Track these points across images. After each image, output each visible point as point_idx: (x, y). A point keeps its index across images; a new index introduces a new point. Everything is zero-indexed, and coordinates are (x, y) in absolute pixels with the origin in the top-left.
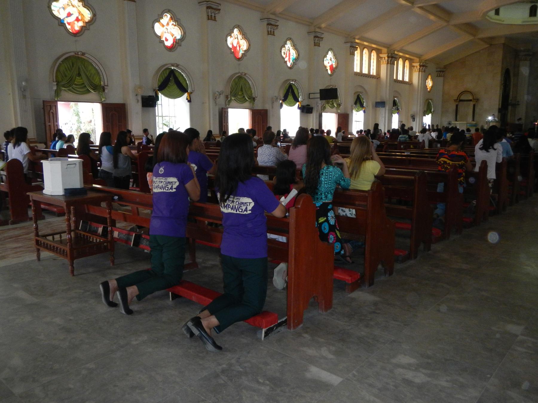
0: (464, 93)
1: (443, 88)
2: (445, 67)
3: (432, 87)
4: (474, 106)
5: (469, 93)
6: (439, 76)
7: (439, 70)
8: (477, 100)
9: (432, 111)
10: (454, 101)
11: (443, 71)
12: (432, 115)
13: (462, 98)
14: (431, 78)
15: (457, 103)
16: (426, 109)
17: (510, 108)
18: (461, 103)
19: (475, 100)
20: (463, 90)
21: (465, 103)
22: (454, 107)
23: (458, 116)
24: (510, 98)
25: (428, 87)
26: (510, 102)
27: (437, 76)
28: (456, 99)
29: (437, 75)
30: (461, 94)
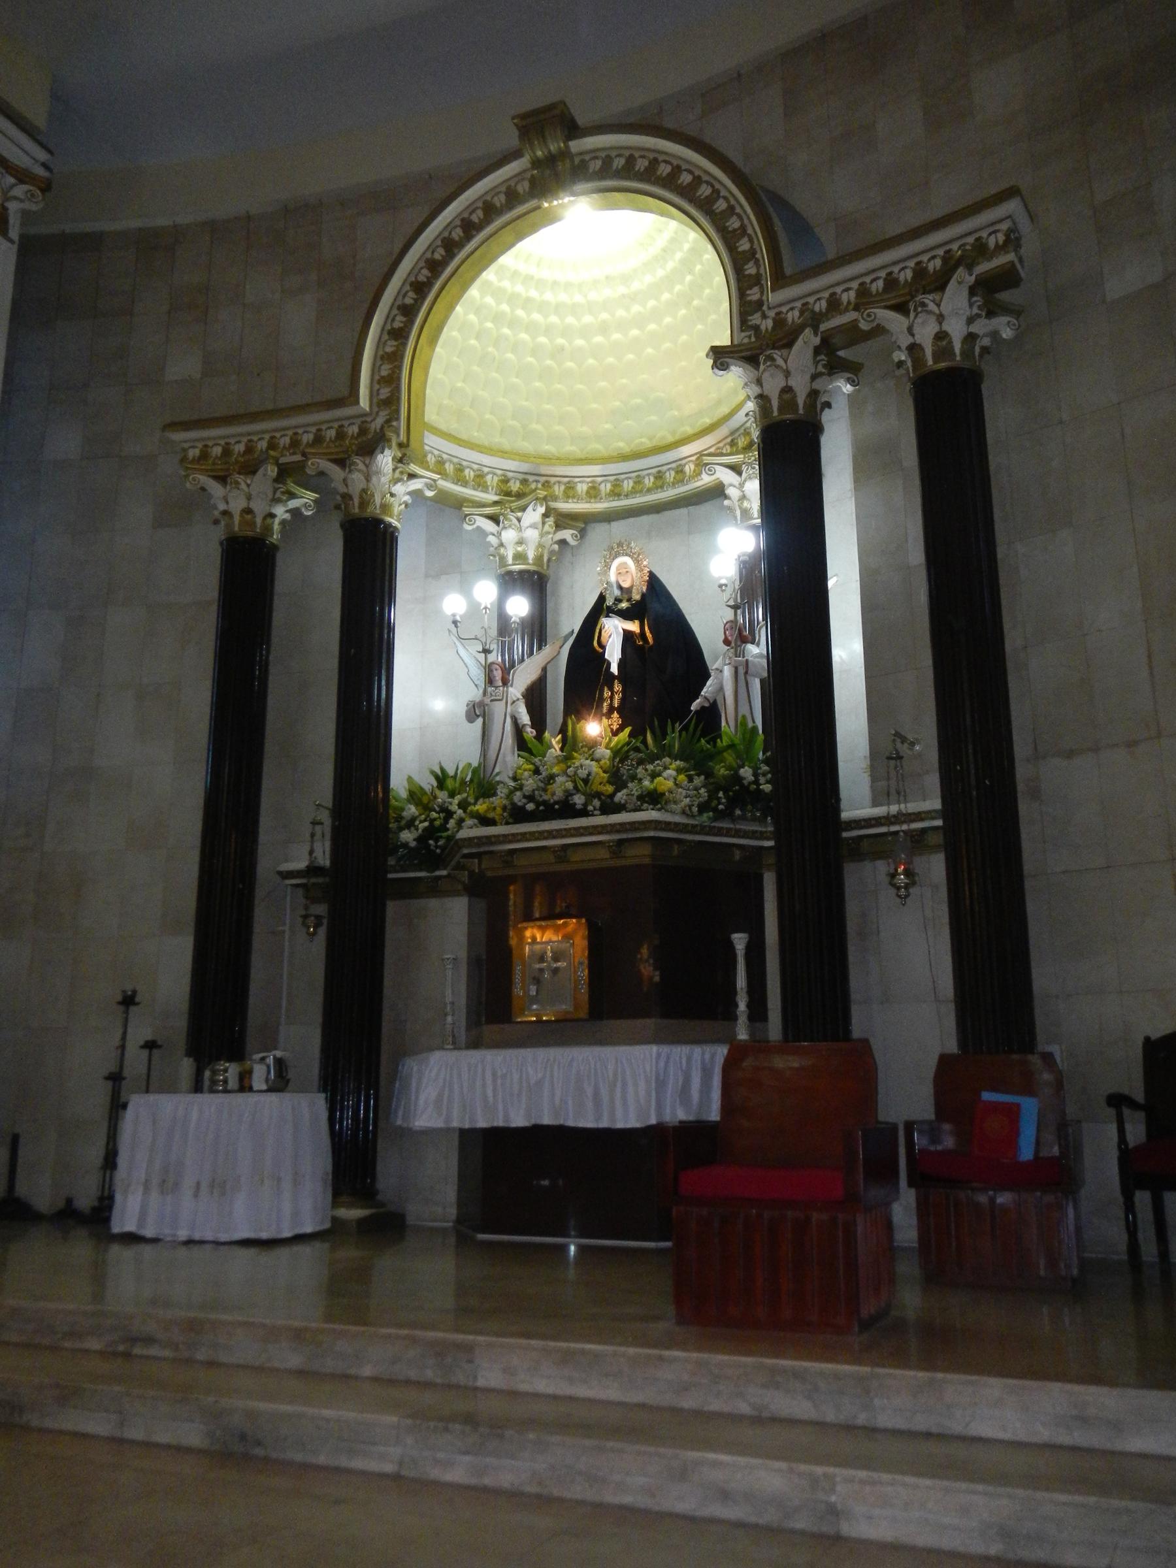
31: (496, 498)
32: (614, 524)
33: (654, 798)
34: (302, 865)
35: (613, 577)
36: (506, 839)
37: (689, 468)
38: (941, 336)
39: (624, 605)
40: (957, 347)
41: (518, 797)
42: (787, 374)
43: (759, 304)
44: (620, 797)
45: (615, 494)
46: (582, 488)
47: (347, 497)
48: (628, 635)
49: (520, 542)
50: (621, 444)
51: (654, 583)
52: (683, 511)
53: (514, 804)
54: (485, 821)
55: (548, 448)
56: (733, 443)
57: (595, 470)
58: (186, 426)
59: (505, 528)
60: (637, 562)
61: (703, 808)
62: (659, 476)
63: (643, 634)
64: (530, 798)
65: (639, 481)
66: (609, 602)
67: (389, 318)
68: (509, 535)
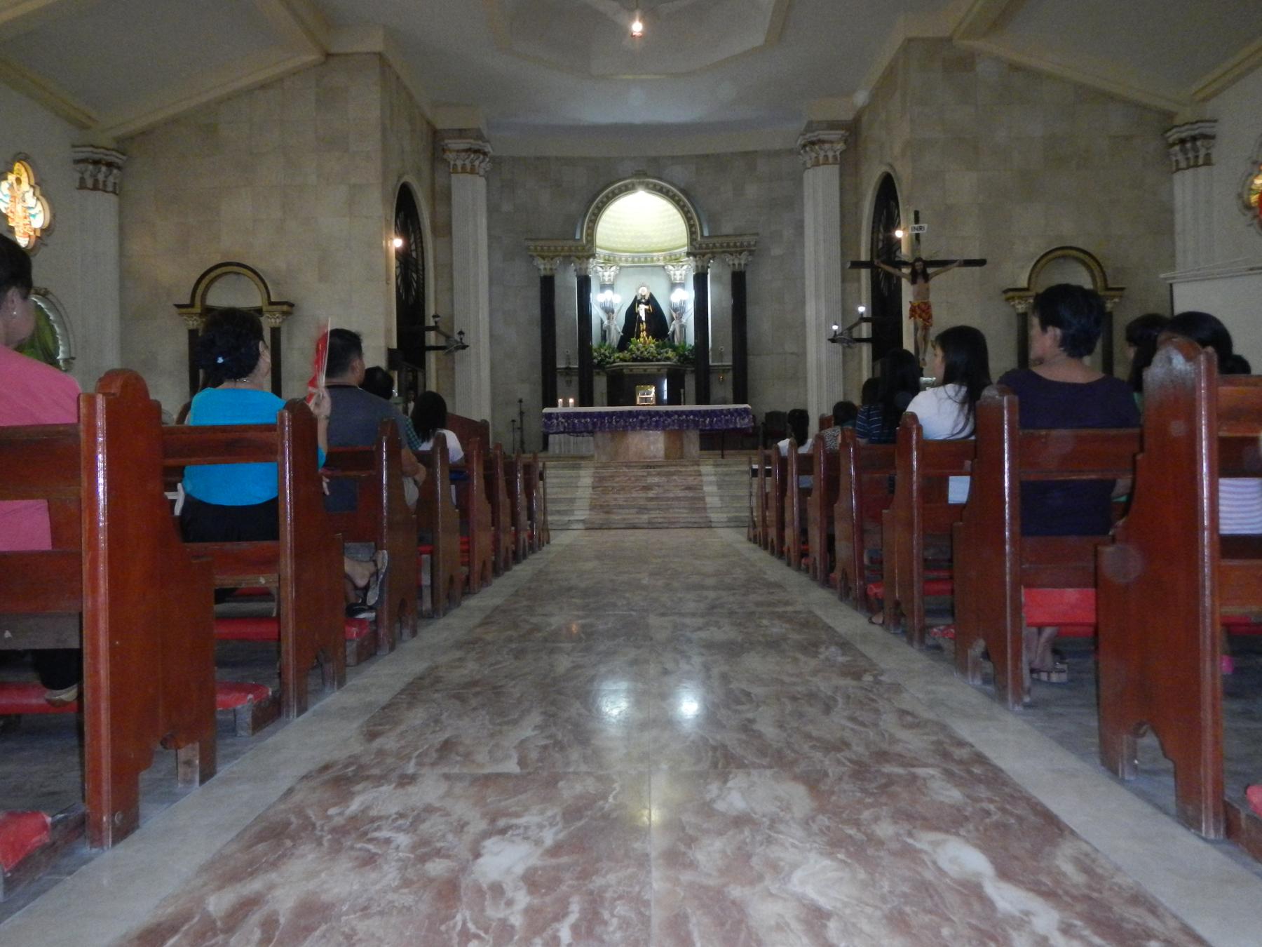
0: (226, 273)
1: (122, 253)
2: (124, 144)
3: (46, 231)
6: (90, 183)
7: (86, 153)
8: (285, 308)
9: (61, 356)
10: (175, 308)
11: (110, 165)
17: (431, 359)
20: (218, 260)
24: (431, 309)
26: (431, 322)
27: (82, 186)
28: (187, 302)
29: (82, 180)
33: (668, 359)
34: (563, 366)
35: (640, 292)
36: (631, 366)
37: (655, 258)
38: (740, 264)
39: (643, 301)
42: (703, 261)
43: (696, 240)
44: (659, 357)
46: (623, 259)
47: (580, 269)
48: (646, 310)
49: (610, 276)
50: (633, 246)
51: (651, 296)
53: (633, 358)
56: (670, 256)
57: (628, 254)
61: (679, 360)
62: (646, 259)
64: (638, 356)
65: (639, 258)
66: (639, 298)
68: (605, 273)
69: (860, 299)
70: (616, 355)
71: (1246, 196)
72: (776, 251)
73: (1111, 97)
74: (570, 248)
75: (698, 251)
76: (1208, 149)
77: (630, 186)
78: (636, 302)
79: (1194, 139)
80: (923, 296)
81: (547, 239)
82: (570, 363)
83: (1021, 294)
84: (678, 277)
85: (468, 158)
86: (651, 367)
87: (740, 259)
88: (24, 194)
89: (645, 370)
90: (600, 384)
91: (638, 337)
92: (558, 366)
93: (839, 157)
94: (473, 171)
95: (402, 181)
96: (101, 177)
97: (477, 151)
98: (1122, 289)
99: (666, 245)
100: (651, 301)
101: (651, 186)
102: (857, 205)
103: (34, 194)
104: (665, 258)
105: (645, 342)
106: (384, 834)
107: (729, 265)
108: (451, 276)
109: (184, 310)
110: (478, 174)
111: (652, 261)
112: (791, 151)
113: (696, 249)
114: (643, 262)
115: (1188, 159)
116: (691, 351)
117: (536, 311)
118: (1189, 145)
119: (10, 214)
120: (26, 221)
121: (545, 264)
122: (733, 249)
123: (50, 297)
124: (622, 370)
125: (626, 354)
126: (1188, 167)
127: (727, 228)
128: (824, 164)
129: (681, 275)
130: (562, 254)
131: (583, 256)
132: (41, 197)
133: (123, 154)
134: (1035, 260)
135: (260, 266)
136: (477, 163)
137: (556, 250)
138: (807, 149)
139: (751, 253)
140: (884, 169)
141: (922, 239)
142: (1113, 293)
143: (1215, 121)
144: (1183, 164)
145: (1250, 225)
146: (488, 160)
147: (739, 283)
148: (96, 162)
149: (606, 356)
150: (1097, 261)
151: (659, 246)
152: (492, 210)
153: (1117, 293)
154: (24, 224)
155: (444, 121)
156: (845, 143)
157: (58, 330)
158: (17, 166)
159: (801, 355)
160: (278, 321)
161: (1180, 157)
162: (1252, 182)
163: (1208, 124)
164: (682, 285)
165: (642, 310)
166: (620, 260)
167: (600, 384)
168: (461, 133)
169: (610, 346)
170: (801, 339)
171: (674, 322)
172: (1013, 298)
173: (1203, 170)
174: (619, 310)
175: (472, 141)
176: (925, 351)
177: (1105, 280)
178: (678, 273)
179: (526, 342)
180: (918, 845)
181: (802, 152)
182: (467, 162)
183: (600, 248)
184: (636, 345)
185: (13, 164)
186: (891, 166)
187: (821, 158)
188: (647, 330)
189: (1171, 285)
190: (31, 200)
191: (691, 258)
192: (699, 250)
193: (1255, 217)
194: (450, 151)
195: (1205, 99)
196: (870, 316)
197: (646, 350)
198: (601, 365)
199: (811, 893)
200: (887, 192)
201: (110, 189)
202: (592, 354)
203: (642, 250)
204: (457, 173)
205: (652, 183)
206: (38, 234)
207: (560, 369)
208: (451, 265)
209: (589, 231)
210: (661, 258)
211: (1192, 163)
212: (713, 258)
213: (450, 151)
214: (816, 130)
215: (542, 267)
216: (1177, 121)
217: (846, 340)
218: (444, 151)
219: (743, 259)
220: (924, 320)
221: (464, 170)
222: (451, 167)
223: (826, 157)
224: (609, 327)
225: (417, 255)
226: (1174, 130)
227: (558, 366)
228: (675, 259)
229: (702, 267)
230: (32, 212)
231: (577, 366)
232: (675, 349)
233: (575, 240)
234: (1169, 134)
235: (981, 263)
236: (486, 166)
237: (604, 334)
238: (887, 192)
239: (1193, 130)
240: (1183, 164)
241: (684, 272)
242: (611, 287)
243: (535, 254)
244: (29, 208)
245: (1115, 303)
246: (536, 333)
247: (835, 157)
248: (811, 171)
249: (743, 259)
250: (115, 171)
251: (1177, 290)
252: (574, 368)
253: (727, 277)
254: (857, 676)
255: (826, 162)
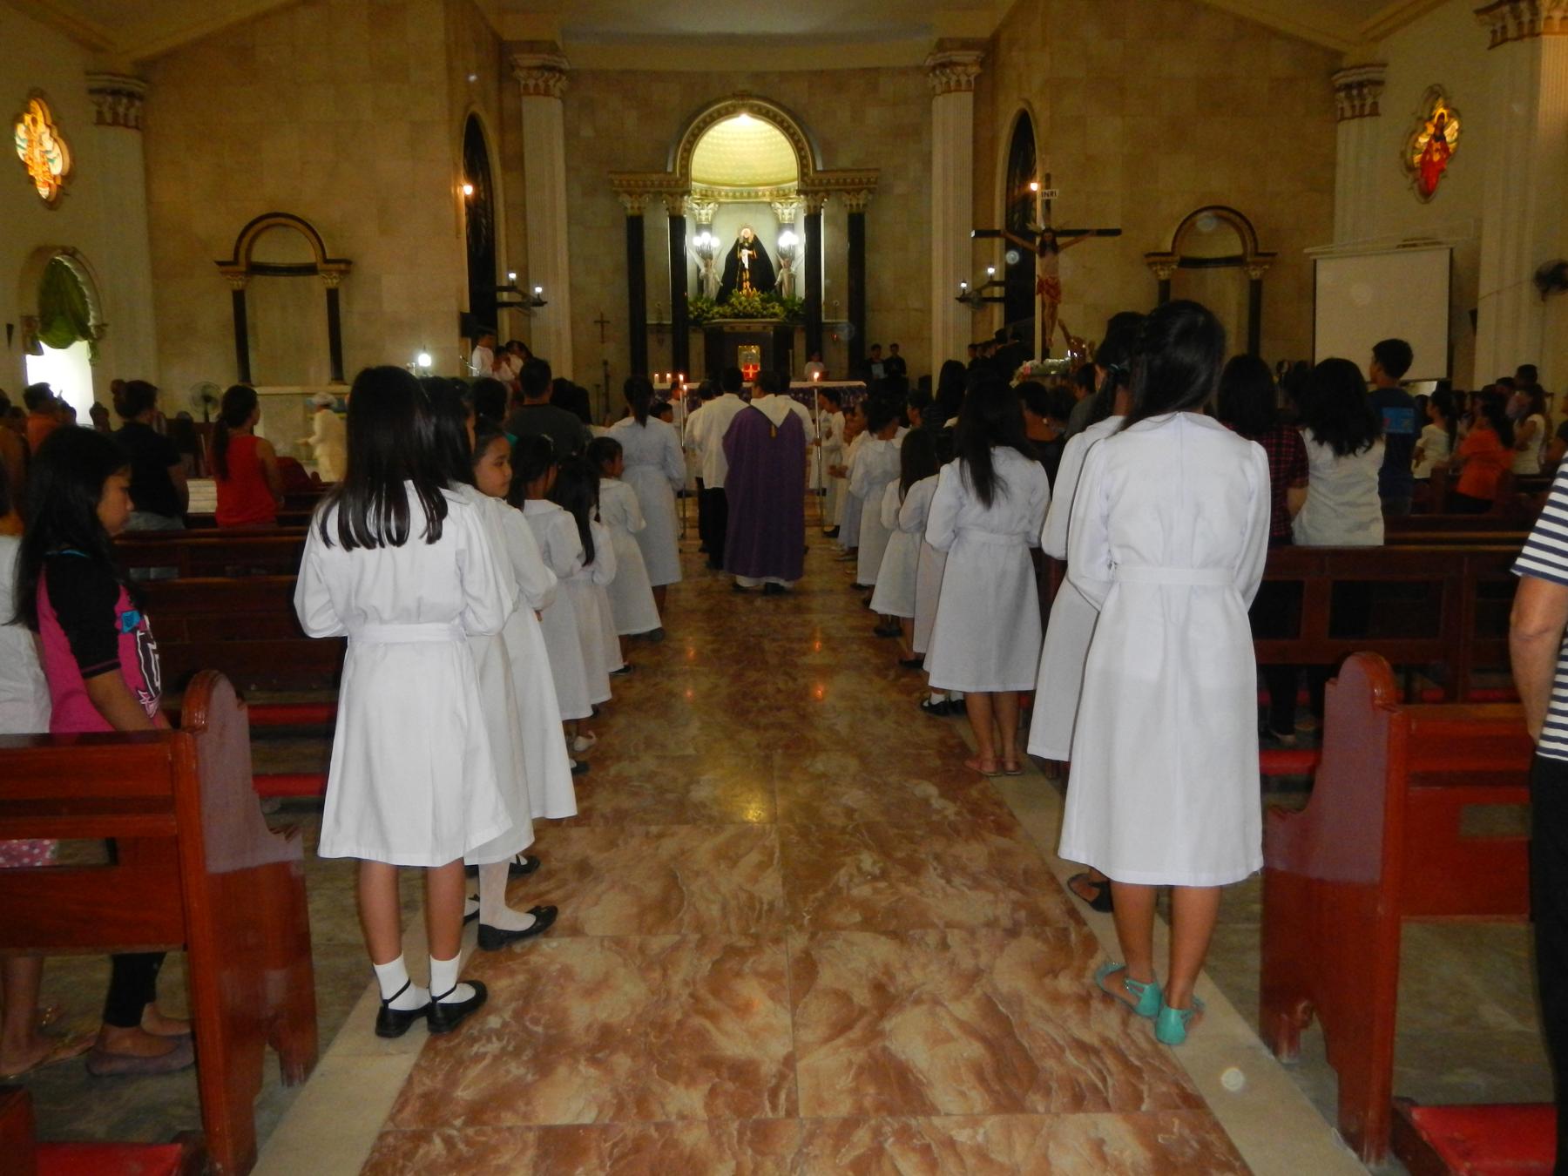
1: (149, 200)
2: (146, 68)
3: (68, 177)
4: (333, 296)
5: (300, 226)
6: (108, 117)
7: (102, 82)
8: (343, 266)
9: (91, 322)
11: (131, 95)
12: (93, 348)
13: (267, 251)
14: (55, 123)
15: (238, 284)
16: (33, 308)
18: (259, 279)
19: (331, 266)
20: (260, 209)
21: (283, 281)
22: (229, 309)
23: (253, 357)
25: (36, 171)
27: (100, 121)
28: (229, 257)
29: (100, 113)
30: (251, 233)
31: (698, 197)
32: (730, 205)
33: (775, 315)
35: (742, 234)
37: (760, 193)
38: (858, 205)
39: (746, 244)
40: (861, 206)
41: (736, 311)
44: (765, 312)
45: (734, 197)
48: (749, 255)
49: (707, 214)
51: (755, 238)
52: (753, 205)
53: (735, 313)
54: (724, 316)
55: (712, 178)
56: (778, 191)
57: (728, 188)
58: (616, 173)
59: (702, 209)
60: (751, 231)
61: (787, 317)
62: (749, 194)
63: (753, 255)
64: (740, 312)
65: (742, 194)
66: (741, 241)
67: (685, 145)
68: (702, 211)
69: (992, 256)
70: (716, 309)
71: (1409, 155)
72: (900, 188)
73: (1274, 33)
74: (661, 185)
75: (809, 188)
76: (1375, 97)
77: (731, 109)
78: (738, 246)
79: (1361, 85)
80: (1053, 269)
81: (631, 172)
82: (662, 319)
83: (1163, 259)
84: (787, 217)
85: (542, 76)
86: (756, 325)
87: (858, 199)
88: (40, 137)
89: (748, 328)
90: (697, 343)
91: (741, 289)
92: (649, 322)
93: (973, 83)
94: (547, 93)
95: (469, 113)
96: (121, 110)
97: (552, 69)
98: (1273, 255)
99: (773, 178)
100: (756, 245)
101: (756, 109)
102: (993, 141)
103: (51, 135)
104: (771, 194)
105: (748, 294)
106: (636, 784)
107: (846, 206)
108: (524, 218)
109: (230, 268)
110: (553, 95)
111: (757, 196)
112: (918, 69)
113: (807, 185)
114: (746, 197)
115: (1353, 107)
116: (802, 305)
117: (622, 256)
118: (1355, 92)
119: (29, 162)
120: (45, 168)
121: (632, 202)
122: (851, 187)
123: (78, 256)
124: (721, 327)
125: (727, 309)
126: (1353, 117)
127: (844, 161)
128: (956, 90)
129: (790, 214)
130: (652, 190)
131: (677, 193)
132: (58, 139)
133: (145, 81)
134: (1182, 220)
135: (313, 217)
136: (551, 83)
137: (645, 186)
138: (938, 72)
139: (871, 191)
140: (1022, 105)
141: (1052, 205)
142: (1261, 259)
143: (1385, 65)
144: (1348, 113)
145: (1412, 188)
146: (564, 78)
147: (856, 228)
148: (115, 93)
149: (704, 311)
150: (1247, 222)
151: (766, 178)
152: (570, 134)
153: (1269, 259)
154: (43, 172)
155: (515, 29)
156: (981, 66)
157: (87, 292)
158: (34, 105)
159: (927, 310)
160: (335, 281)
161: (1346, 105)
162: (1417, 140)
163: (1376, 69)
164: (792, 227)
165: (745, 255)
166: (719, 194)
167: (697, 343)
168: (532, 46)
169: (707, 300)
170: (927, 292)
171: (782, 271)
172: (1155, 263)
173: (1367, 120)
174: (720, 254)
175: (546, 56)
176: (1052, 331)
177: (1256, 247)
178: (786, 211)
179: (611, 295)
180: (907, 785)
181: (931, 75)
182: (541, 83)
183: (696, 181)
184: (738, 298)
185: (28, 103)
186: (1029, 104)
187: (952, 84)
188: (750, 280)
189: (1315, 261)
190: (48, 144)
191: (802, 196)
192: (812, 186)
193: (1416, 180)
194: (521, 68)
195: (1376, 39)
196: (1003, 279)
197: (750, 304)
198: (697, 322)
199: (850, 803)
200: (1024, 129)
201: (133, 123)
202: (688, 308)
203: (743, 183)
204: (529, 94)
205: (756, 105)
206: (59, 182)
207: (652, 325)
208: (524, 205)
209: (683, 162)
210: (767, 193)
211: (1357, 112)
212: (828, 193)
213: (521, 68)
214: (950, 50)
215: (629, 205)
216: (1344, 64)
217: (975, 301)
218: (513, 68)
219: (862, 199)
220: (1052, 297)
221: (538, 94)
222: (522, 87)
223: (958, 82)
224: (706, 276)
225: (485, 195)
226: (1341, 74)
227: (649, 322)
228: (783, 195)
229: (815, 207)
230: (50, 156)
231: (670, 322)
232: (782, 303)
233: (666, 172)
234: (1335, 77)
235: (1117, 232)
236: (563, 83)
237: (701, 283)
238: (1024, 129)
239: (1360, 74)
240: (1348, 113)
241: (793, 211)
242: (709, 227)
243: (620, 190)
244: (47, 152)
245: (1265, 269)
246: (622, 283)
247: (969, 81)
248: (941, 98)
249: (862, 199)
250: (137, 103)
251: (1320, 265)
252: (670, 325)
253: (843, 219)
254: (909, 694)
255: (958, 88)
